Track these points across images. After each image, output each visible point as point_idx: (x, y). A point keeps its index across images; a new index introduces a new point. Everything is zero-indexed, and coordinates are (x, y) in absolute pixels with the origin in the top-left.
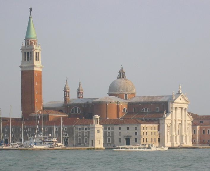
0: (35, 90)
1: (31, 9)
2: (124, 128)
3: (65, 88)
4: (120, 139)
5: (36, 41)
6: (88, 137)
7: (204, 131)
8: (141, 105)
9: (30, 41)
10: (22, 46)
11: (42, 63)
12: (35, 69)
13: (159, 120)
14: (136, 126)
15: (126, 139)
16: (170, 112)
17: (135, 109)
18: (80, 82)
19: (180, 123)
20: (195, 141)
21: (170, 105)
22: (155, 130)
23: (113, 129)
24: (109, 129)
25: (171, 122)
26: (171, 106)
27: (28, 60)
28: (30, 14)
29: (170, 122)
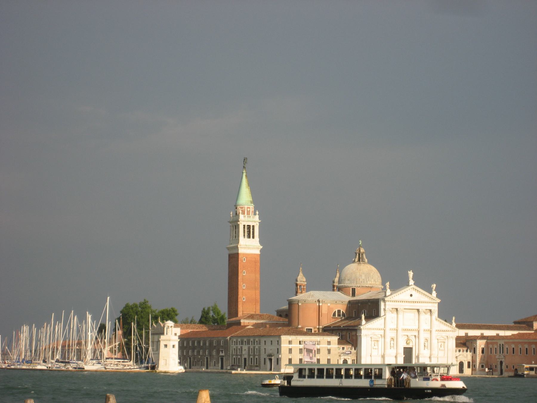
0: (240, 283)
1: (245, 159)
2: (268, 340)
5: (248, 208)
6: (241, 355)
8: (360, 306)
9: (238, 208)
11: (261, 242)
12: (241, 251)
16: (380, 317)
17: (355, 311)
19: (417, 334)
20: (474, 365)
22: (329, 346)
23: (260, 344)
25: (383, 333)
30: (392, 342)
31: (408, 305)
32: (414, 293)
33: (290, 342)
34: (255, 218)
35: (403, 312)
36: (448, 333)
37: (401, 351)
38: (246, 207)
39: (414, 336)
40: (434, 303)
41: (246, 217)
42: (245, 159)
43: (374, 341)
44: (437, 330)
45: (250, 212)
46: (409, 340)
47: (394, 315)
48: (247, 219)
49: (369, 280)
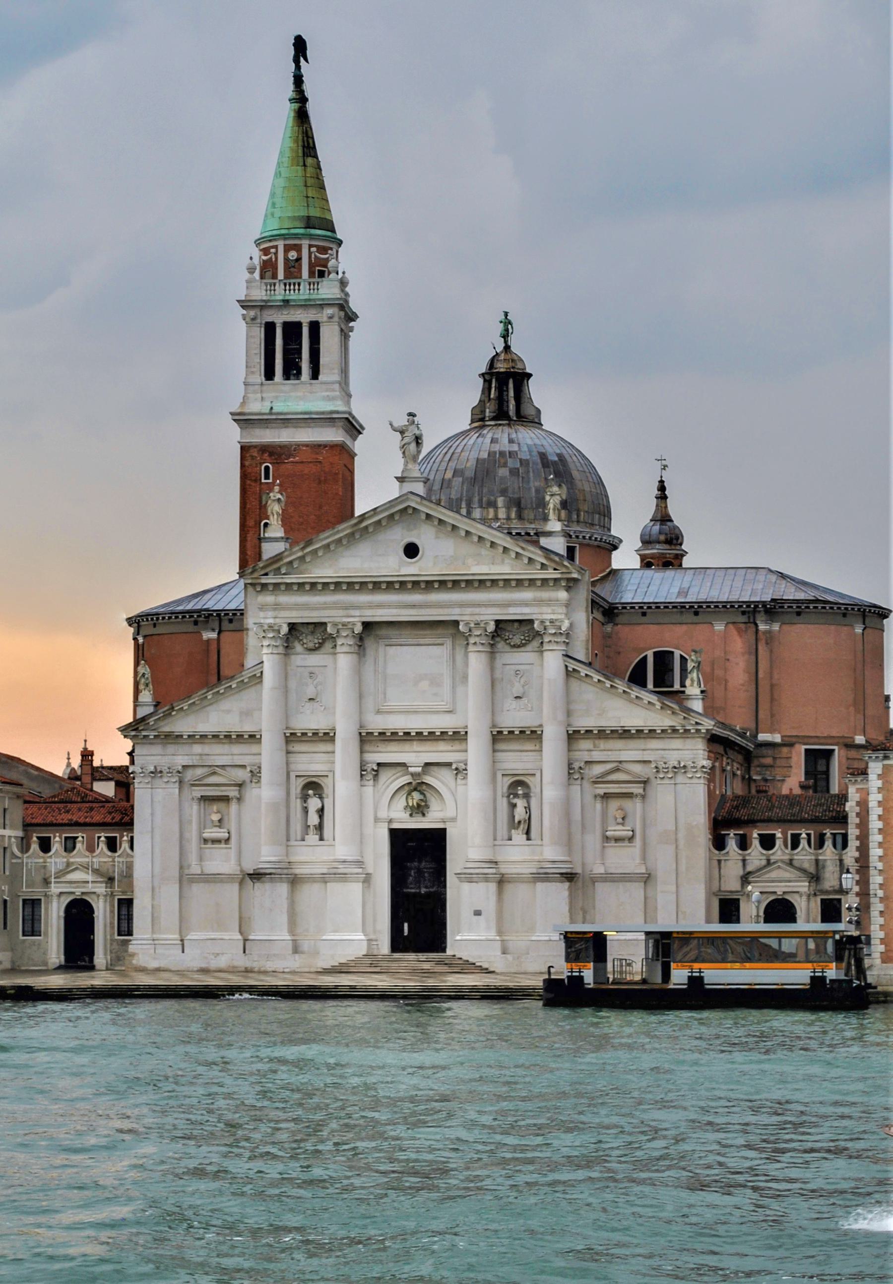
1: (300, 46)
5: (287, 249)
18: (662, 488)
30: (314, 804)
32: (424, 537)
34: (320, 291)
36: (654, 744)
38: (281, 244)
39: (446, 775)
40: (545, 581)
41: (279, 288)
42: (300, 46)
43: (204, 799)
44: (576, 732)
45: (300, 265)
46: (415, 789)
48: (281, 298)
49: (480, 501)
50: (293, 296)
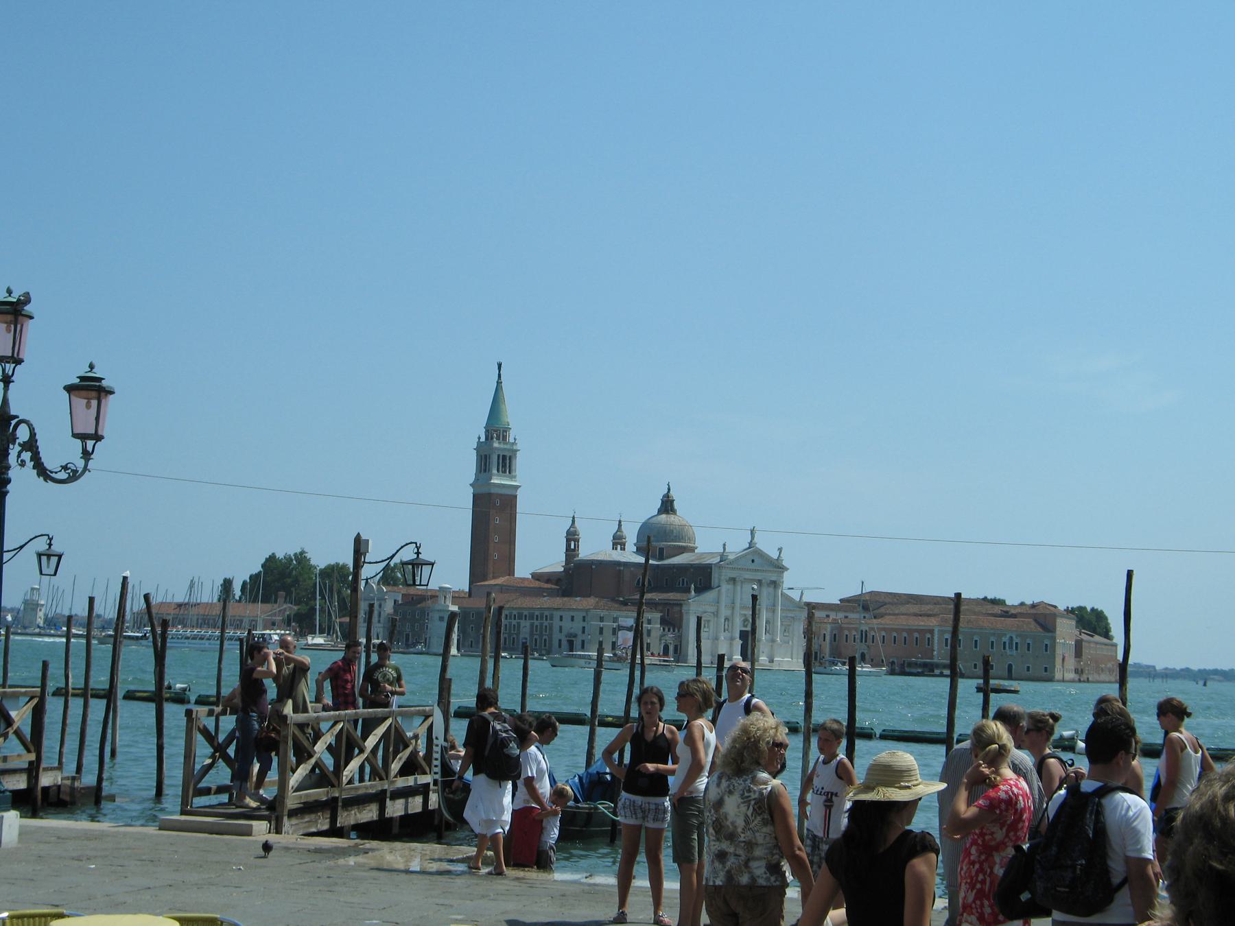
1: (500, 366)
2: (566, 615)
3: (568, 533)
4: (560, 641)
5: (503, 431)
6: (518, 634)
7: (847, 635)
10: (479, 443)
12: (493, 491)
13: (681, 605)
14: (584, 614)
15: (568, 641)
16: (713, 589)
21: (715, 576)
23: (552, 619)
24: (546, 616)
26: (716, 576)
27: (485, 471)
28: (499, 376)
29: (712, 609)
31: (748, 575)
33: (602, 619)
35: (742, 582)
37: (737, 635)
38: (501, 430)
47: (730, 587)
50: (505, 447)
